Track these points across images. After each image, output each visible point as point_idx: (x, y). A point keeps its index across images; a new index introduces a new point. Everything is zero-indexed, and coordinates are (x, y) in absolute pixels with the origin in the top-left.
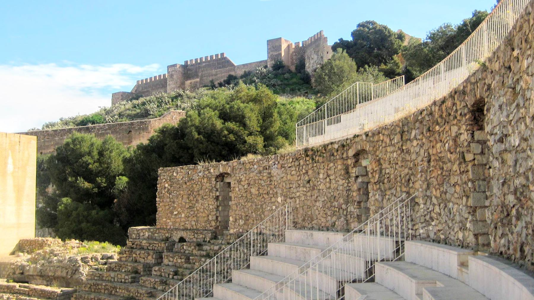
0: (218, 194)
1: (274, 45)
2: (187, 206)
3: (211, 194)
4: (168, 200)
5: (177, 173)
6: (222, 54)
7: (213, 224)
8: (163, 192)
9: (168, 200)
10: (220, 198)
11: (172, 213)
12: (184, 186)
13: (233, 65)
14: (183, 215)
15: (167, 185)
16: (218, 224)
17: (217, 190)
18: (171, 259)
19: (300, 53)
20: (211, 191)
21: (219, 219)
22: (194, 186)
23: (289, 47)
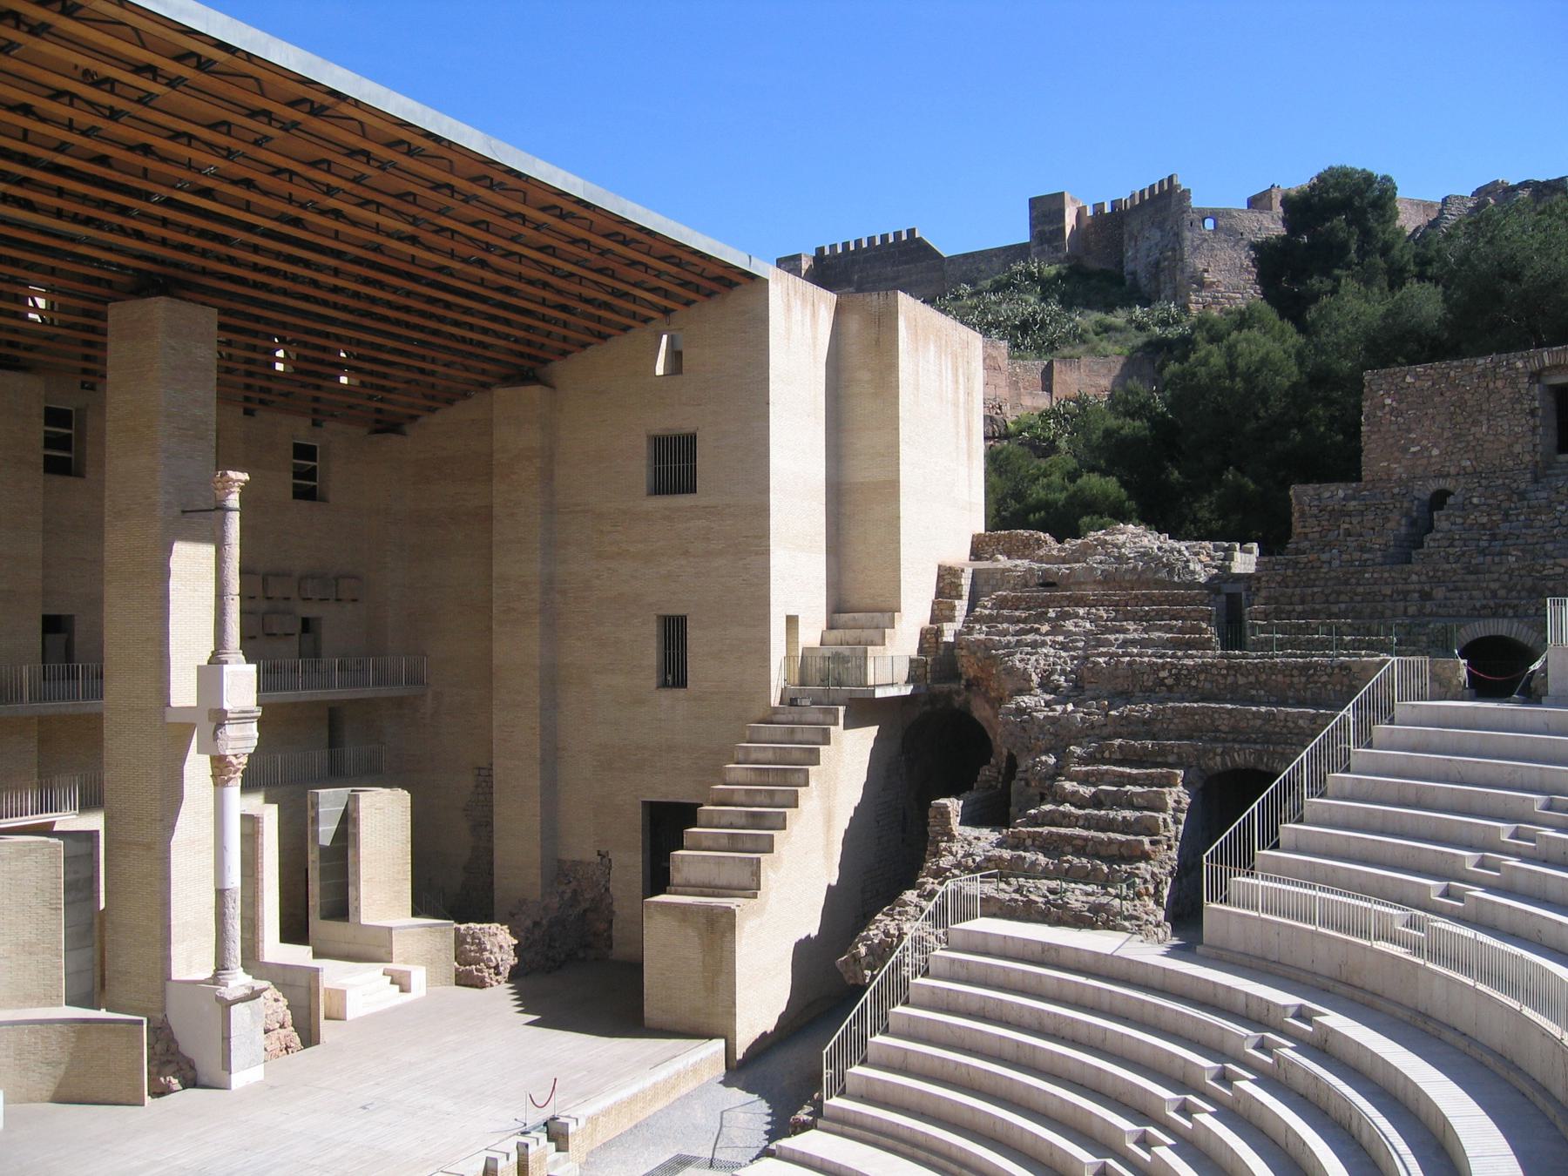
0: (1537, 404)
1: (1046, 211)
2: (1446, 434)
3: (1518, 406)
4: (1393, 428)
5: (1417, 377)
6: (911, 232)
7: (1527, 458)
8: (1379, 414)
9: (1393, 428)
10: (1540, 412)
11: (1405, 450)
12: (1437, 399)
13: (938, 256)
14: (1435, 452)
15: (1388, 401)
16: (1538, 458)
17: (1533, 399)
18: (1459, 520)
19: (1111, 225)
20: (1518, 401)
21: (1540, 448)
22: (1467, 396)
23: (1080, 214)
